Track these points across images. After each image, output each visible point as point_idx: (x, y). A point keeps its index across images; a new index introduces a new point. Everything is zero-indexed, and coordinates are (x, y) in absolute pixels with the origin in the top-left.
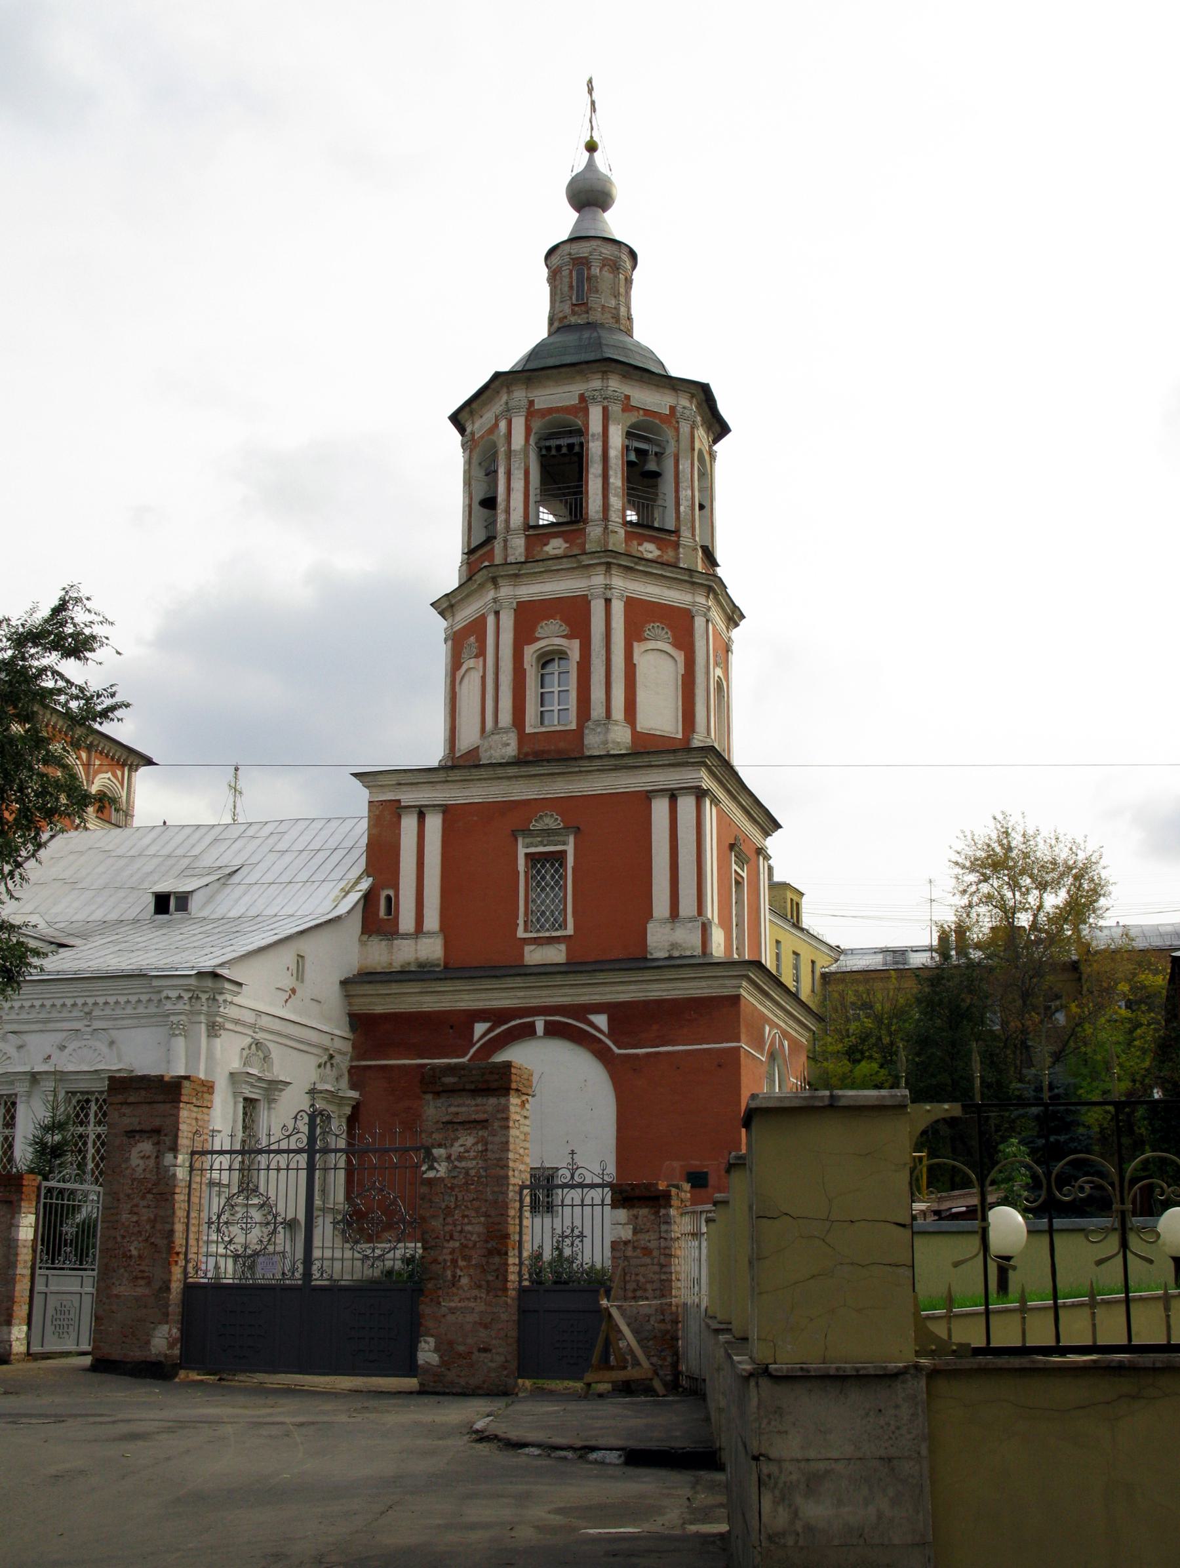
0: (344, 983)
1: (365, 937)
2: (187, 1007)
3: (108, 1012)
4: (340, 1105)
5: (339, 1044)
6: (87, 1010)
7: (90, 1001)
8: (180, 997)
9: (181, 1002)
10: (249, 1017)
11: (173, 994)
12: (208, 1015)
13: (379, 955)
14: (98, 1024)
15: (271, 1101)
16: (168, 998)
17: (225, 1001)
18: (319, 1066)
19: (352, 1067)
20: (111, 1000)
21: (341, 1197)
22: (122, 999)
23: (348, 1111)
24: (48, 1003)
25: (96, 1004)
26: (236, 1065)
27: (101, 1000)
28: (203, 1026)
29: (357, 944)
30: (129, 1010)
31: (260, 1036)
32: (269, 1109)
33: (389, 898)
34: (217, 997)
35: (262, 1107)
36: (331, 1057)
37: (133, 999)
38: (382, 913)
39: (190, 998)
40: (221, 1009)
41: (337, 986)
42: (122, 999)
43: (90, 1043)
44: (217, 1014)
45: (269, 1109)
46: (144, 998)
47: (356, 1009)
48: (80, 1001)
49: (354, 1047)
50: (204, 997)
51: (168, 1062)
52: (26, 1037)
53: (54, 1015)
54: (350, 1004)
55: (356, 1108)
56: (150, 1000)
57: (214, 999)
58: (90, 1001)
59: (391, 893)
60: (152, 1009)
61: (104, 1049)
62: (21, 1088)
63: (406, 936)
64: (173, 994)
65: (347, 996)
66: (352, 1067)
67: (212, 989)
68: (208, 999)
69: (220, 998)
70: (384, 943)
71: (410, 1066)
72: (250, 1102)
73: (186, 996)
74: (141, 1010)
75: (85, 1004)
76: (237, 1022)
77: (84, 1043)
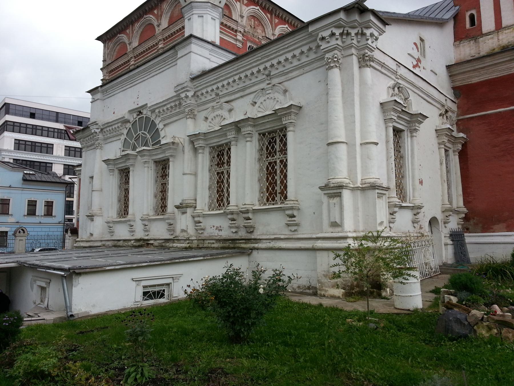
0: (449, 67)
1: (457, 43)
2: (339, 42)
3: (281, 69)
4: (453, 143)
5: (450, 104)
6: (267, 72)
7: (268, 65)
8: (333, 34)
9: (334, 39)
10: (392, 65)
11: (326, 34)
12: (358, 49)
13: (468, 50)
14: (275, 81)
15: (413, 131)
16: (323, 39)
17: (372, 35)
18: (440, 115)
19: (458, 120)
20: (282, 59)
21: (461, 203)
22: (289, 56)
23: (460, 147)
24: (242, 75)
25: (272, 66)
26: (385, 97)
27: (275, 62)
28: (355, 59)
29: (452, 48)
30: (296, 63)
31: (400, 81)
32: (412, 137)
33: (472, 17)
34: (365, 31)
35: (406, 135)
36: (447, 111)
37: (297, 52)
38: (468, 26)
39: (341, 34)
40: (369, 42)
41: (445, 69)
42: (289, 56)
43: (271, 95)
44: (367, 47)
45: (412, 137)
46: (305, 49)
47: (458, 84)
48: (261, 67)
49: (458, 108)
50: (353, 32)
51: (327, 94)
52: (233, 104)
53: (248, 82)
54: (453, 82)
55: (464, 145)
56: (310, 49)
57: (363, 34)
58: (268, 65)
59: (474, 12)
60: (312, 56)
61: (280, 97)
62: (231, 135)
63: (487, 34)
64: (326, 34)
65: (450, 76)
66: (458, 120)
67: (360, 24)
68: (357, 34)
69: (368, 32)
70: (472, 42)
71: (506, 111)
72: (397, 132)
73: (337, 32)
74: (304, 59)
75: (265, 69)
76: (383, 65)
77: (268, 96)
